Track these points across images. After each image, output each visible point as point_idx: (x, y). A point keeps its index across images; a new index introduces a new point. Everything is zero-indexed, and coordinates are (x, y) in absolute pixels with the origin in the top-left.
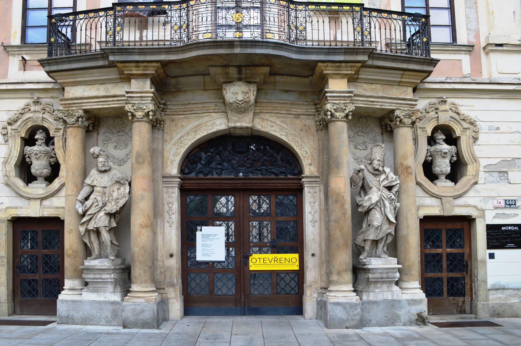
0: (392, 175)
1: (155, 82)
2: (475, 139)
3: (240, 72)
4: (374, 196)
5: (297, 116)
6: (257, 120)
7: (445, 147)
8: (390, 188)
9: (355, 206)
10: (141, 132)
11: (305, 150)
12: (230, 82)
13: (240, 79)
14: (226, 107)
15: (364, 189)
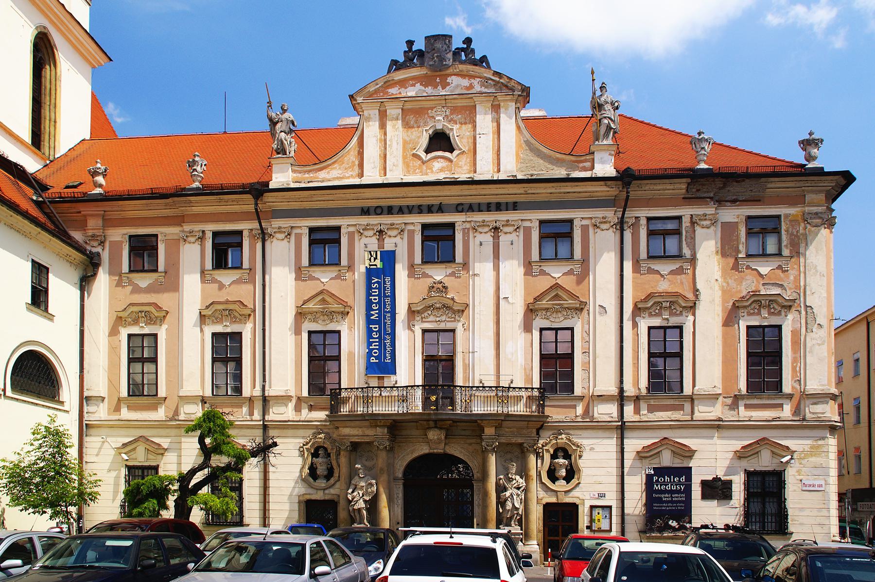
0: (521, 481)
1: (388, 427)
2: (580, 457)
3: (436, 424)
4: (508, 494)
5: (470, 444)
6: (447, 447)
7: (561, 461)
8: (518, 488)
9: (498, 497)
10: (382, 456)
11: (474, 464)
12: (429, 428)
13: (436, 427)
14: (428, 442)
15: (505, 489)
